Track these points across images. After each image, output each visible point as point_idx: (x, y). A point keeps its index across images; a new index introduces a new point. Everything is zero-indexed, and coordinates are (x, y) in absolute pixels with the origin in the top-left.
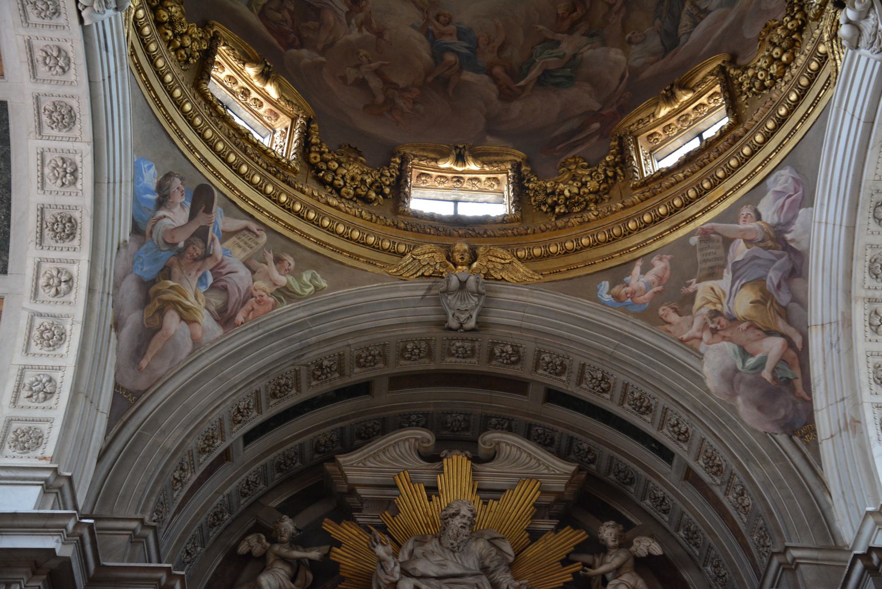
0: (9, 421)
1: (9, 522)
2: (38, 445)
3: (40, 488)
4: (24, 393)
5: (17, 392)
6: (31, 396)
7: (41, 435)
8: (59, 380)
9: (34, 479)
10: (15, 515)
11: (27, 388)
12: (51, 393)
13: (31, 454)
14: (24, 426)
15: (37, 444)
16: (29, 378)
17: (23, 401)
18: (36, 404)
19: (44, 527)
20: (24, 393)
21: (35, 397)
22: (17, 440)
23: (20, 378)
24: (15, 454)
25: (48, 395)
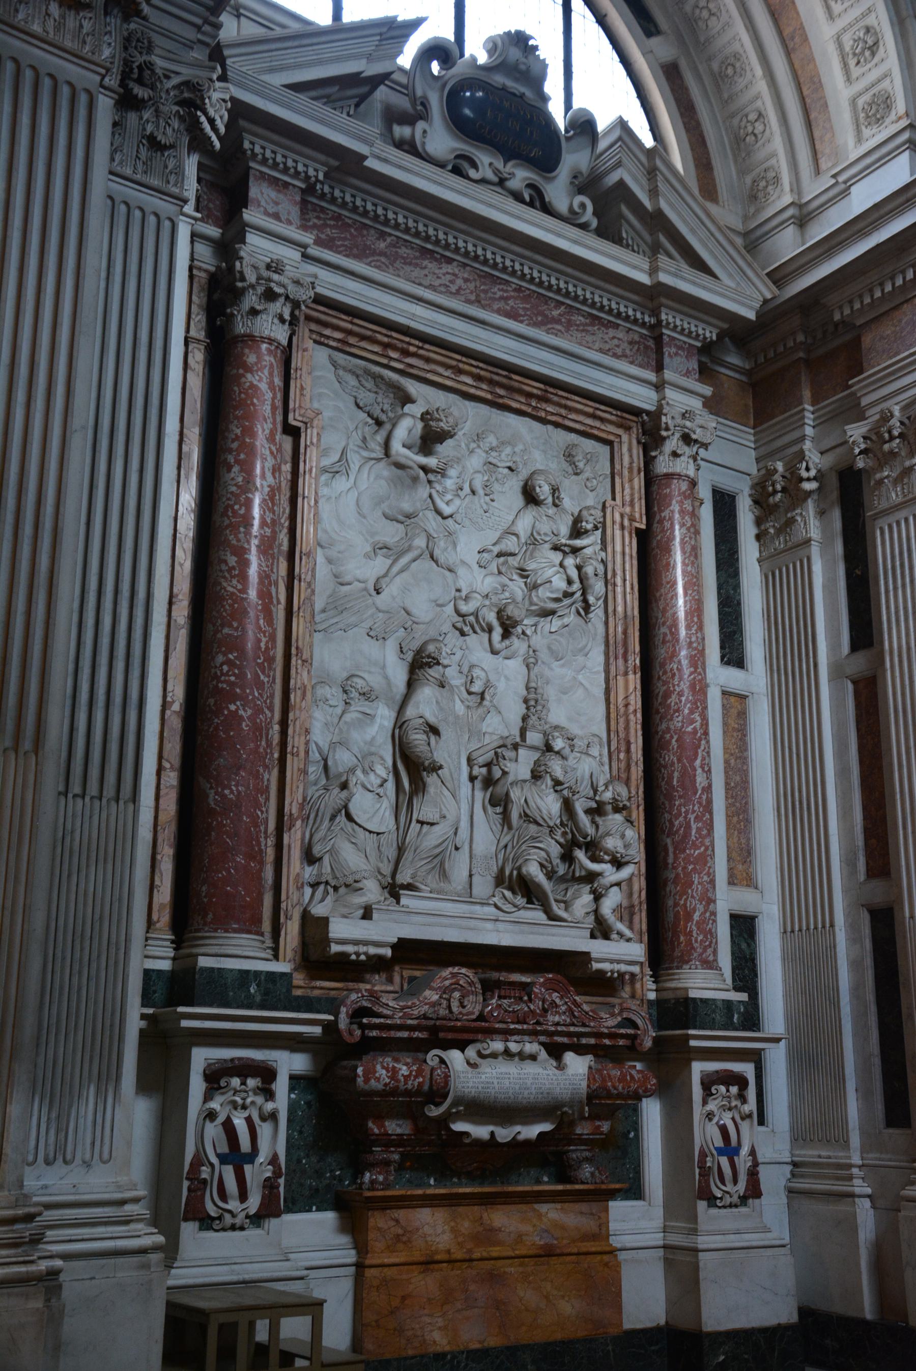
0: (853, 102)
1: (876, 215)
2: (889, 107)
3: (907, 153)
4: (852, 62)
5: (845, 66)
6: (858, 63)
7: (886, 95)
8: (875, 24)
9: (898, 147)
10: (876, 206)
11: (851, 56)
12: (875, 44)
13: (888, 121)
14: (867, 97)
15: (888, 107)
16: (848, 44)
17: (855, 72)
18: (869, 66)
19: (908, 201)
20: (852, 62)
21: (862, 60)
22: (868, 117)
23: (841, 50)
24: (874, 131)
25: (873, 49)
